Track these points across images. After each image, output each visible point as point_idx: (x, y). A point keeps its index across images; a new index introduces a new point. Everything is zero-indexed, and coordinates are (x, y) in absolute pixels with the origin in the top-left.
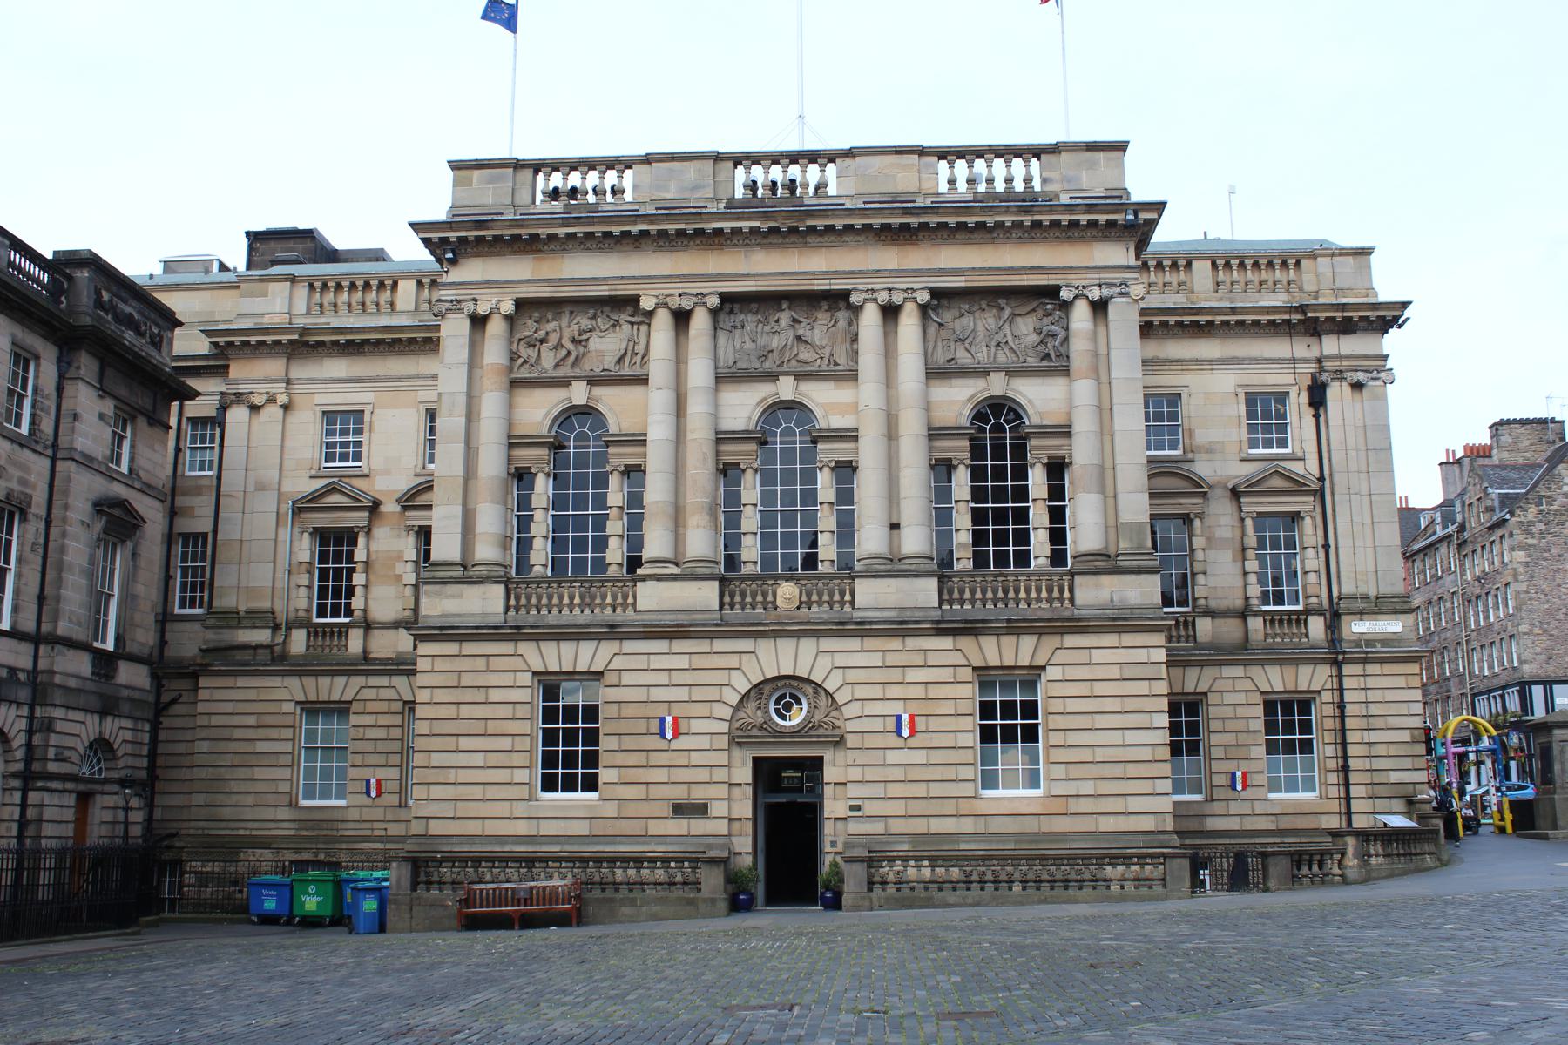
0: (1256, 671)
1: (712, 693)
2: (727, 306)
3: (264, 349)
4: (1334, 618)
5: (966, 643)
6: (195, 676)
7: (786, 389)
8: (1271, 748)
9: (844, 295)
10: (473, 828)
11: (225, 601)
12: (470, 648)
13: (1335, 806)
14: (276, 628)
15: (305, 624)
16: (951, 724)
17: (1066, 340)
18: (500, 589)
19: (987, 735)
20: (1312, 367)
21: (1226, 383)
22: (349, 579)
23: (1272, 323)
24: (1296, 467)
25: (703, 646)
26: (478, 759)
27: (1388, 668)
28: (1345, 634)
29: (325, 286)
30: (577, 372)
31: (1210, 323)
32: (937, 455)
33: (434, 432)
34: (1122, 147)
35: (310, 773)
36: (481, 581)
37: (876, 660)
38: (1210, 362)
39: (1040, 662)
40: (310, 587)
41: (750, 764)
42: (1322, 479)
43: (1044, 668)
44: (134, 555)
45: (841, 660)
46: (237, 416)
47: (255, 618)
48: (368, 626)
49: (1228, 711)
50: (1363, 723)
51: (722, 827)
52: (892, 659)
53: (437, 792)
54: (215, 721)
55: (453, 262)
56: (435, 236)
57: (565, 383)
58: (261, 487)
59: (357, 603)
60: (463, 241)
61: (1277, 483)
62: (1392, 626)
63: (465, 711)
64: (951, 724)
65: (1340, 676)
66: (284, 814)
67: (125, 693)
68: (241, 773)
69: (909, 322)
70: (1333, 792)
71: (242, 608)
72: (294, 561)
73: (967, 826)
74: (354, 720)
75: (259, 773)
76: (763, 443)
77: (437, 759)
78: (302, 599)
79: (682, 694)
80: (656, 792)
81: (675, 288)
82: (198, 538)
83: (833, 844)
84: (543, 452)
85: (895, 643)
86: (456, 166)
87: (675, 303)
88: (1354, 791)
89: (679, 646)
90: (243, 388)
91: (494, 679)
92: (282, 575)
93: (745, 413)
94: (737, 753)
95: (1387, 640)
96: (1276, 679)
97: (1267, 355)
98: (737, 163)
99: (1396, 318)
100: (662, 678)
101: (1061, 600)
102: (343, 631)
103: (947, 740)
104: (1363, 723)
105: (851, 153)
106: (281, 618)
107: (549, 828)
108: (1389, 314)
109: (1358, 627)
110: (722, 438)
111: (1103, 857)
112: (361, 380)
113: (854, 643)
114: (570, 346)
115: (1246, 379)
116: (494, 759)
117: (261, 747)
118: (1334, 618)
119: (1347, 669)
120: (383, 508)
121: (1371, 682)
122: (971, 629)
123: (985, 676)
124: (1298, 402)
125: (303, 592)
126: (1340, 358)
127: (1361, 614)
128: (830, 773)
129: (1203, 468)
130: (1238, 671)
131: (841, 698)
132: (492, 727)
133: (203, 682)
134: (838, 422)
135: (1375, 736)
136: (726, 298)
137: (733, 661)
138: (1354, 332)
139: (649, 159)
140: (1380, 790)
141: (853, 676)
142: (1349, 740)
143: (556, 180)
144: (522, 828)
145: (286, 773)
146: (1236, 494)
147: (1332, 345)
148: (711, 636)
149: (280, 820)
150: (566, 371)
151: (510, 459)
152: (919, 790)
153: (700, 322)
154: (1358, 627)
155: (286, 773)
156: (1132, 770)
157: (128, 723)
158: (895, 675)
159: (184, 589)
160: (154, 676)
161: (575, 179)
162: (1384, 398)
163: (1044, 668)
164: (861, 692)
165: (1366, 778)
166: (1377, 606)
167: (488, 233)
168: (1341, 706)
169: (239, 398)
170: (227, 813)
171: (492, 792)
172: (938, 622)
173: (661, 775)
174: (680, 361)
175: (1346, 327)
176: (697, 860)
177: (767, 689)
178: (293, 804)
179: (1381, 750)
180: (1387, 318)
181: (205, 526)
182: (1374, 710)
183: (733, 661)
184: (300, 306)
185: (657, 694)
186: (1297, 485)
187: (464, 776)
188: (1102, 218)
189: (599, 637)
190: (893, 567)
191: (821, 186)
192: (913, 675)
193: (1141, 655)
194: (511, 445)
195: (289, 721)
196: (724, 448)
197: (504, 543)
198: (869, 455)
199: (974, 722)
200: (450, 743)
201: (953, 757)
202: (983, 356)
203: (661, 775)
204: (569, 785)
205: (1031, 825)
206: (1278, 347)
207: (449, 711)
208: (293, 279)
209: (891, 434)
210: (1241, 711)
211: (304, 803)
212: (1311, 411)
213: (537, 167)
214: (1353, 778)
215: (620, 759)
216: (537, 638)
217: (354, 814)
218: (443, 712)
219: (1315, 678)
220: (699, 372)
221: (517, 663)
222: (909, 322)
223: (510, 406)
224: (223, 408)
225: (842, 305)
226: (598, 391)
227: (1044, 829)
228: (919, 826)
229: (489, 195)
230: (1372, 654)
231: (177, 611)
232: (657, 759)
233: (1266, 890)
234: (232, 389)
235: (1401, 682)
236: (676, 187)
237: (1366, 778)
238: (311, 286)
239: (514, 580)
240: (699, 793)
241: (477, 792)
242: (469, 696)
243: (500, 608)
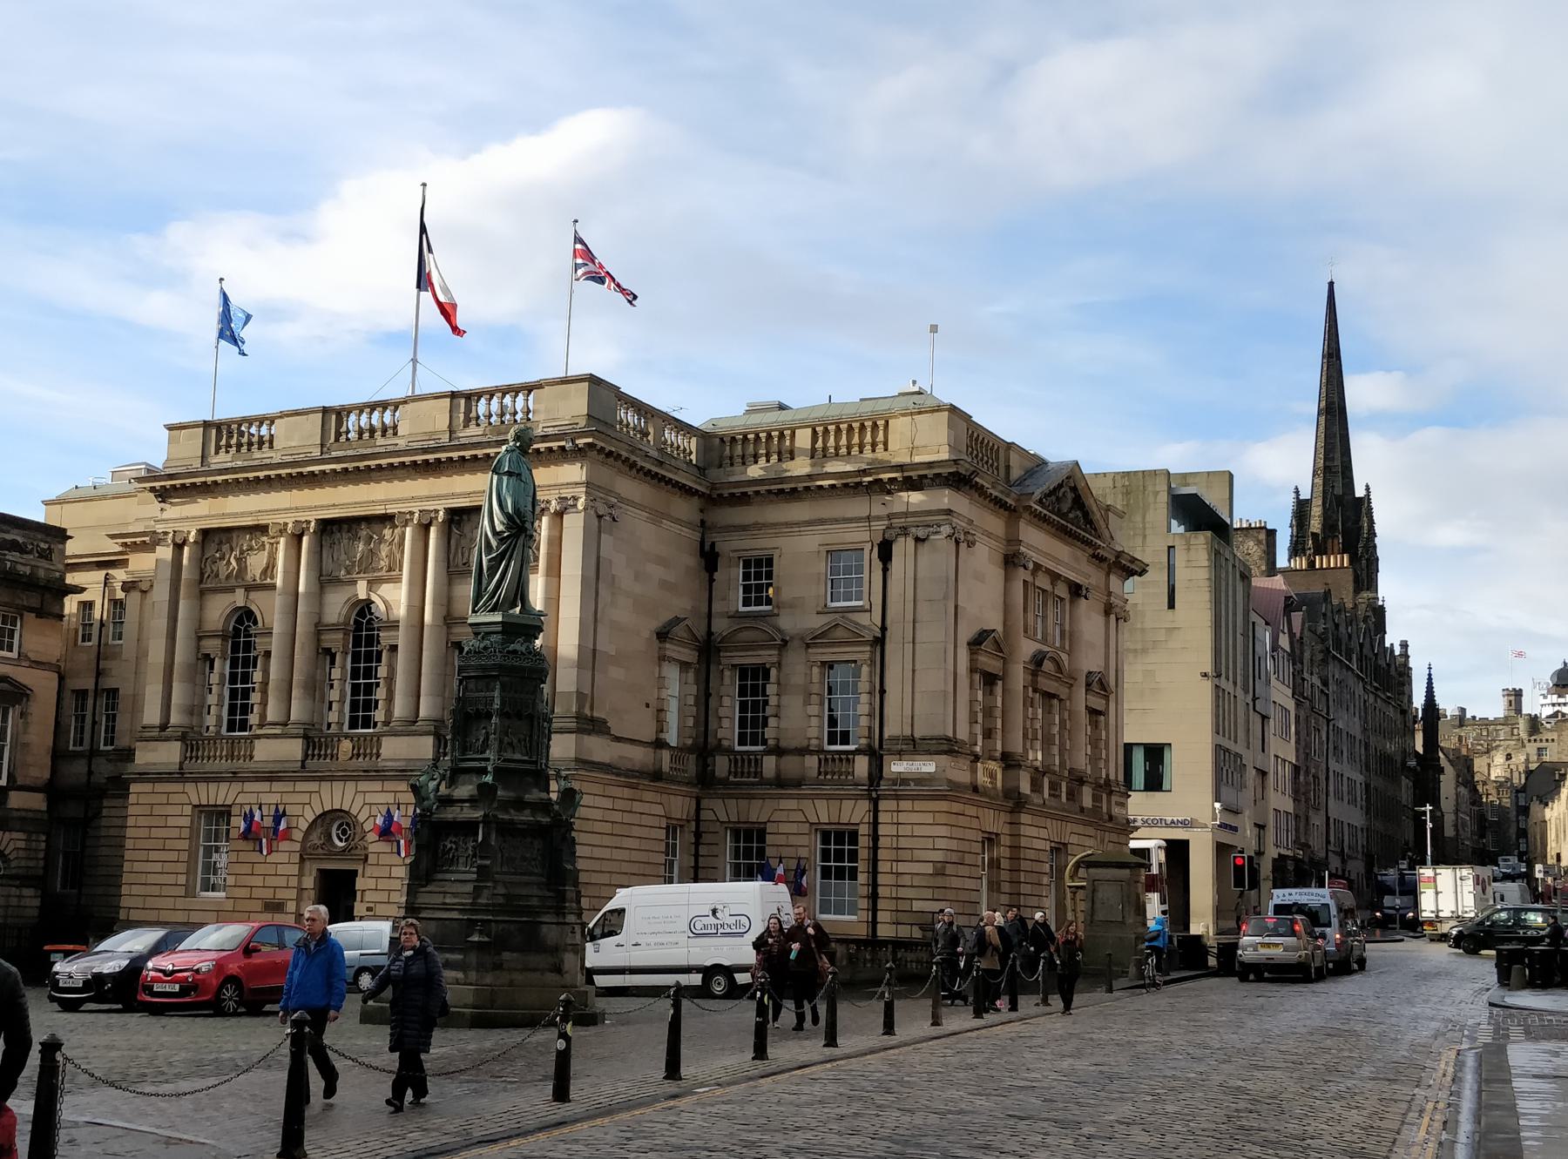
0: (807, 805)
4: (876, 756)
8: (826, 873)
12: (160, 787)
21: (811, 541)
23: (846, 485)
24: (863, 619)
25: (288, 786)
26: (158, 867)
27: (919, 805)
31: (794, 490)
38: (798, 524)
41: (314, 873)
44: (22, 715)
45: (370, 798)
49: (781, 840)
57: (232, 590)
61: (839, 634)
62: (927, 766)
65: (876, 811)
67: (15, 814)
80: (257, 893)
82: (113, 693)
86: (170, 428)
88: (881, 916)
89: (277, 786)
95: (921, 780)
96: (823, 812)
97: (849, 515)
109: (897, 767)
113: (377, 786)
119: (883, 805)
121: (903, 818)
124: (871, 556)
127: (900, 754)
128: (360, 883)
129: (788, 623)
130: (792, 804)
135: (902, 867)
137: (305, 798)
142: (880, 869)
148: (294, 780)
150: (233, 582)
151: (198, 648)
154: (897, 767)
157: (21, 835)
160: (51, 802)
165: (892, 905)
166: (913, 746)
173: (258, 881)
179: (906, 880)
182: (903, 843)
183: (305, 798)
194: (200, 638)
203: (258, 881)
206: (858, 507)
210: (793, 840)
214: (881, 904)
216: (196, 781)
219: (855, 812)
221: (183, 799)
226: (253, 595)
230: (908, 789)
232: (259, 869)
235: (929, 818)
237: (892, 905)
239: (191, 740)
240: (281, 894)
241: (155, 890)
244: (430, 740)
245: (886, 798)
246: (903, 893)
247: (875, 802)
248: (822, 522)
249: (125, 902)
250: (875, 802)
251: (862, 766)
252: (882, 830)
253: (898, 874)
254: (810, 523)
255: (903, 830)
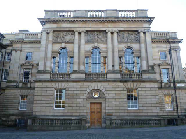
1: (84, 92)
2: (87, 32)
3: (18, 43)
4: (174, 83)
5: (125, 84)
6: (4, 90)
7: (96, 45)
9: (105, 31)
10: (43, 114)
11: (10, 79)
13: (176, 111)
14: (17, 83)
15: (22, 82)
16: (123, 97)
17: (139, 38)
18: (50, 74)
19: (129, 99)
20: (169, 48)
22: (29, 76)
24: (168, 62)
26: (45, 102)
27: (183, 91)
28: (176, 86)
29: (28, 34)
30: (63, 42)
32: (119, 55)
33: (41, 56)
34: (147, 10)
35: (21, 105)
36: (47, 73)
37: (111, 87)
38: (155, 47)
39: (137, 87)
40: (23, 77)
42: (171, 63)
43: (138, 88)
45: (105, 87)
46: (13, 52)
47: (14, 82)
48: (31, 83)
50: (179, 99)
51: (85, 114)
52: (113, 87)
53: (37, 107)
54: (7, 97)
55: (44, 25)
56: (42, 20)
58: (16, 63)
59: (30, 79)
60: (46, 21)
63: (43, 94)
64: (123, 97)
65: (176, 92)
66: (17, 111)
68: (10, 105)
69: (115, 35)
70: (175, 109)
71: (12, 80)
72: (20, 73)
73: (126, 114)
74: (28, 97)
75: (13, 105)
76: (92, 53)
77: (38, 102)
78: (22, 79)
79: (79, 92)
81: (79, 29)
82: (7, 70)
83: (104, 117)
84: (57, 54)
85: (114, 84)
86: (45, 11)
87: (79, 31)
90: (15, 48)
91: (48, 89)
92: (19, 75)
93: (89, 48)
94: (87, 101)
98: (89, 12)
99: (181, 41)
100: (76, 89)
101: (140, 78)
102: (27, 84)
103: (122, 100)
104: (179, 99)
105: (106, 10)
106: (18, 82)
107: (56, 114)
108: (180, 41)
109: (178, 85)
110: (86, 52)
111: (150, 120)
112: (32, 48)
114: (62, 38)
115: (160, 50)
116: (47, 102)
117: (14, 101)
118: (174, 83)
119: (177, 91)
120: (34, 66)
121: (180, 93)
122: (126, 82)
123: (128, 89)
124: (167, 53)
125: (22, 78)
126: (173, 47)
127: (178, 83)
131: (105, 93)
132: (47, 97)
133: (6, 91)
134: (104, 50)
135: (181, 101)
136: (87, 31)
138: (175, 43)
139: (75, 11)
140: (182, 109)
141: (107, 89)
143: (61, 14)
144: (51, 114)
145: (17, 105)
146: (159, 65)
147: (172, 45)
149: (16, 112)
152: (118, 108)
153: (83, 34)
154: (178, 85)
155: (17, 105)
156: (153, 105)
158: (114, 89)
159: (4, 77)
161: (64, 14)
162: (179, 53)
163: (138, 88)
164: (108, 92)
166: (180, 82)
167: (50, 20)
168: (176, 96)
169: (14, 50)
170: (8, 111)
171: (47, 108)
172: (121, 81)
174: (80, 40)
175: (174, 42)
176: (81, 120)
177: (92, 91)
178: (18, 110)
180: (180, 41)
181: (8, 68)
184: (24, 37)
185: (74, 92)
186: (168, 64)
187: (42, 105)
188: (145, 20)
189: (65, 82)
190: (114, 72)
191: (102, 15)
192: (117, 89)
193: (154, 86)
195: (18, 97)
196: (86, 54)
197: (51, 67)
198: (110, 55)
199: (127, 97)
200: (40, 99)
201: (123, 103)
202: (126, 40)
203: (75, 105)
204: (60, 107)
205: (136, 114)
206: (164, 45)
207: (40, 94)
208: (23, 34)
209: (113, 52)
211: (20, 109)
212: (169, 54)
213: (58, 12)
214: (178, 107)
215: (68, 102)
217: (27, 111)
218: (39, 94)
220: (83, 41)
221: (52, 86)
222: (115, 35)
223: (52, 47)
224: (12, 51)
225: (105, 32)
227: (139, 115)
228: (118, 114)
229: (49, 16)
230: (180, 88)
231: (3, 80)
232: (74, 102)
233: (177, 125)
234: (13, 48)
236: (79, 14)
238: (26, 34)
241: (44, 108)
242: (43, 92)
243: (49, 78)
244: (120, 74)
245: (178, 90)
246: (182, 105)
247: (175, 90)
248: (159, 47)
249: (34, 111)
250: (175, 90)
251: (172, 85)
252: (177, 95)
253: (180, 102)
254: (157, 47)
255: (180, 95)
